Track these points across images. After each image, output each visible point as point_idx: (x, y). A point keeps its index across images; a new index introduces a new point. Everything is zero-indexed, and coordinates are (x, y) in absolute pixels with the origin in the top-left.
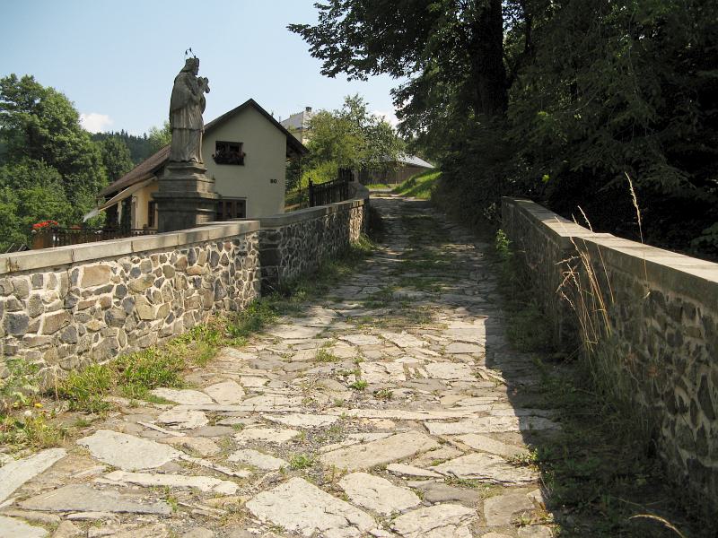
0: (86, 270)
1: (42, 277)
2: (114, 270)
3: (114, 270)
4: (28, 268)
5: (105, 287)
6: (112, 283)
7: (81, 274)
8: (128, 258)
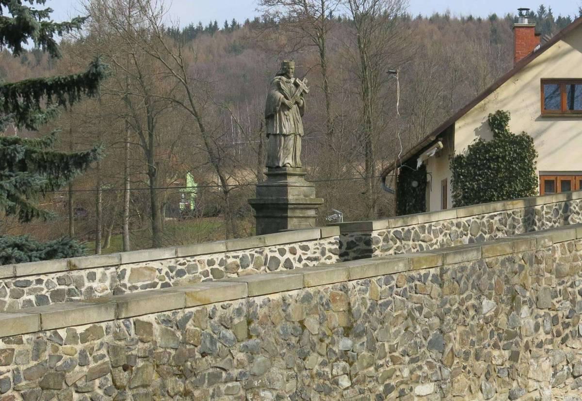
0: (132, 270)
1: (95, 274)
2: (160, 271)
3: (160, 271)
4: (84, 267)
5: (151, 284)
6: (157, 280)
7: (128, 273)
8: (173, 260)
